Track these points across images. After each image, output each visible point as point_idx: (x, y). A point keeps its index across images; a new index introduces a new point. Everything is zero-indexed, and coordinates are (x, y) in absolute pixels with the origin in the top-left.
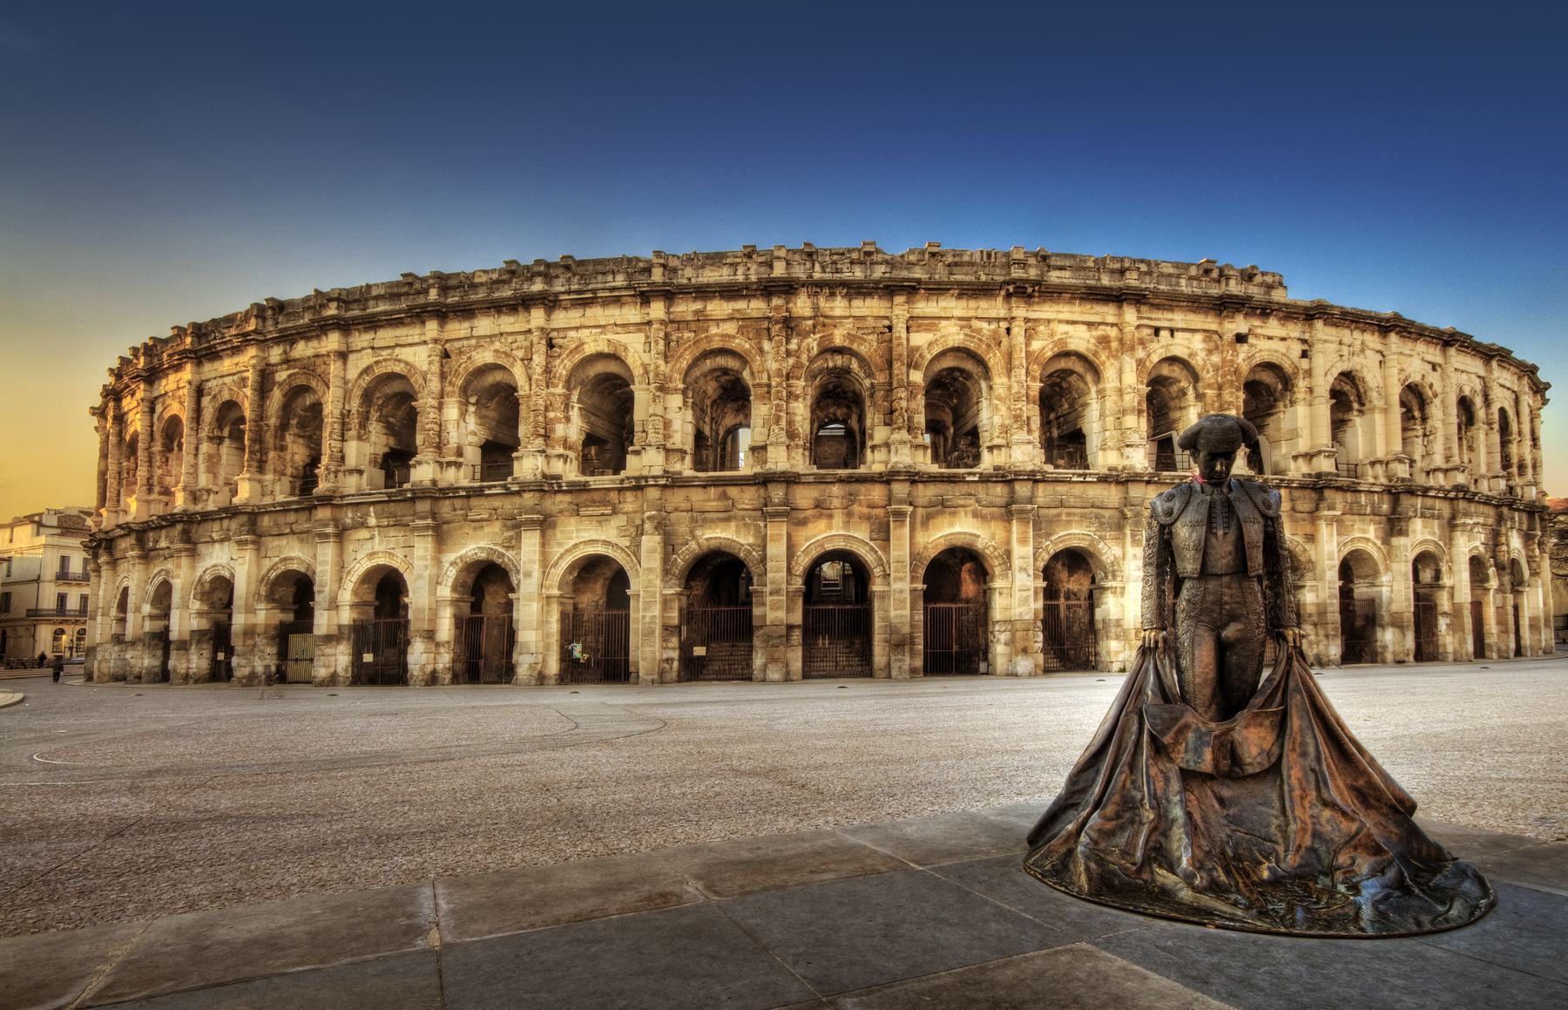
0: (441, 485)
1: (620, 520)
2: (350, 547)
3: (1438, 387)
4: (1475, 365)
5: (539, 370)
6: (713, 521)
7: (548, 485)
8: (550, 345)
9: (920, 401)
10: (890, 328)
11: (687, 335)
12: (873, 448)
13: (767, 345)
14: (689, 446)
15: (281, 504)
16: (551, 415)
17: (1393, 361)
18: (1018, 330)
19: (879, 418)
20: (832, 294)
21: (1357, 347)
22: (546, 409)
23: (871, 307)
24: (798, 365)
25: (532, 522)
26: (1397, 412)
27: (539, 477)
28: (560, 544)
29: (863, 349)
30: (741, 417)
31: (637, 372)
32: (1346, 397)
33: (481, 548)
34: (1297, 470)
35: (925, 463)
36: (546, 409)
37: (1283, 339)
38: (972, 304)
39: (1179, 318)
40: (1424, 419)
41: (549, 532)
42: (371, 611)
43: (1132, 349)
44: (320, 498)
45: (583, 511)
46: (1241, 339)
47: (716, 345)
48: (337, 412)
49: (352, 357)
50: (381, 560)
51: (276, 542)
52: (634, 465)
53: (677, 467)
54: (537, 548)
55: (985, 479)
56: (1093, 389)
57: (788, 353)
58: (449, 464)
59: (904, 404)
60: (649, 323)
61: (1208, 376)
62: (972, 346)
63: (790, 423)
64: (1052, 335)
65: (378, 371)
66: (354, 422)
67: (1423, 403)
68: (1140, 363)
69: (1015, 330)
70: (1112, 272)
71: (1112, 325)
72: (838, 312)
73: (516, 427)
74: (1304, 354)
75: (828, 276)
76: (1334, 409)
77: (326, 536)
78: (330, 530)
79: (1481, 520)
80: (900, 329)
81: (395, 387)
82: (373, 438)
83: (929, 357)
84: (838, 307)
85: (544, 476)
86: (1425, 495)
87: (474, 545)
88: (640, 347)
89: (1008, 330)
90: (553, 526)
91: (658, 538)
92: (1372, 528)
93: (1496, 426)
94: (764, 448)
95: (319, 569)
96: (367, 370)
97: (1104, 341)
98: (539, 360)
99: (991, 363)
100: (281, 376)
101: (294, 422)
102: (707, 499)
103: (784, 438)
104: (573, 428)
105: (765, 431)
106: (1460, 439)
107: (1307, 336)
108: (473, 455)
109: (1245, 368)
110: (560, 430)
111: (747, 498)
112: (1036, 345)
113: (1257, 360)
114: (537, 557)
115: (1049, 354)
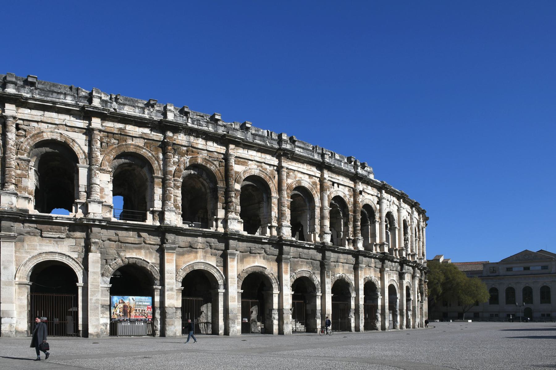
37: (372, 195)
38: (263, 155)
39: (341, 179)
46: (361, 192)
56: (308, 205)
59: (234, 200)
61: (350, 207)
63: (175, 201)
64: (295, 178)
70: (319, 153)
71: (318, 177)
72: (200, 146)
74: (378, 203)
83: (243, 178)
84: (200, 143)
102: (131, 237)
103: (174, 209)
104: (31, 182)
105: (160, 203)
107: (379, 196)
113: (365, 203)
115: (294, 186)
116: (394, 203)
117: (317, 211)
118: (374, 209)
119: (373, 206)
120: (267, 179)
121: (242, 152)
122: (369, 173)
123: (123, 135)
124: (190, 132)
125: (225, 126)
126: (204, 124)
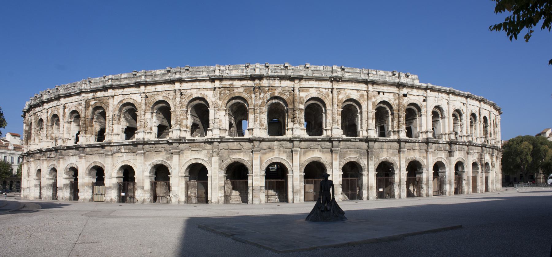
0: (146, 140)
1: (205, 152)
2: (115, 159)
3: (465, 110)
4: (477, 103)
5: (178, 103)
6: (235, 153)
7: (181, 141)
8: (182, 95)
9: (303, 114)
10: (293, 91)
11: (227, 92)
12: (288, 130)
13: (253, 95)
14: (227, 127)
15: (93, 144)
16: (182, 117)
17: (451, 102)
18: (335, 92)
19: (290, 120)
20: (275, 80)
21: (440, 98)
22: (180, 115)
23: (287, 84)
24: (263, 103)
25: (176, 152)
26: (452, 118)
27: (178, 138)
28: (185, 159)
29: (285, 97)
30: (243, 117)
31: (210, 104)
32: (437, 113)
33: (159, 160)
34: (422, 137)
35: (304, 134)
36: (180, 115)
40: (461, 120)
41: (181, 155)
42: (122, 179)
43: (371, 99)
44: (106, 143)
45: (193, 149)
46: (405, 95)
47: (236, 95)
48: (111, 116)
49: (115, 97)
50: (126, 163)
51: (91, 156)
52: (209, 135)
53: (223, 135)
54: (178, 160)
55: (323, 140)
57: (260, 98)
58: (148, 133)
59: (297, 116)
60: (215, 88)
61: (395, 107)
62: (320, 97)
63: (261, 121)
64: (346, 93)
65: (124, 102)
66: (117, 118)
67: (461, 115)
68: (374, 103)
69: (334, 92)
70: (365, 74)
73: (170, 120)
74: (424, 100)
75: (273, 74)
76: (433, 118)
77: (108, 155)
78: (110, 153)
79: (477, 151)
80: (297, 91)
81: (130, 107)
82: (122, 123)
84: (277, 83)
85: (180, 137)
86: (459, 145)
87: (157, 159)
88: (212, 96)
89: (332, 92)
90: (183, 153)
91: (217, 158)
92: (443, 154)
93: (482, 122)
94: (253, 130)
95: (105, 166)
96: (121, 101)
97: (362, 96)
98: (178, 99)
99: (326, 102)
100: (92, 103)
101: (95, 117)
104: (189, 122)
106: (471, 126)
107: (425, 95)
108: (155, 130)
109: (406, 105)
110: (184, 122)
111: (247, 145)
112: (340, 97)
113: (410, 102)
114: (178, 163)
115: (345, 100)
116: (443, 98)
117: (365, 115)
118: (420, 106)
119: (419, 104)
120: (323, 98)
121: (304, 84)
122: (413, 80)
123: (232, 87)
124: (269, 77)
125: (293, 69)
126: (279, 71)
